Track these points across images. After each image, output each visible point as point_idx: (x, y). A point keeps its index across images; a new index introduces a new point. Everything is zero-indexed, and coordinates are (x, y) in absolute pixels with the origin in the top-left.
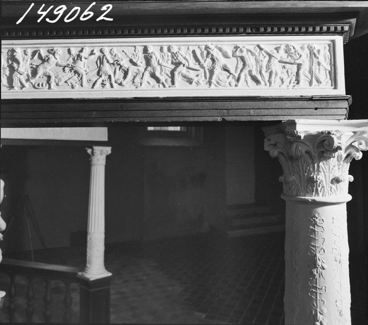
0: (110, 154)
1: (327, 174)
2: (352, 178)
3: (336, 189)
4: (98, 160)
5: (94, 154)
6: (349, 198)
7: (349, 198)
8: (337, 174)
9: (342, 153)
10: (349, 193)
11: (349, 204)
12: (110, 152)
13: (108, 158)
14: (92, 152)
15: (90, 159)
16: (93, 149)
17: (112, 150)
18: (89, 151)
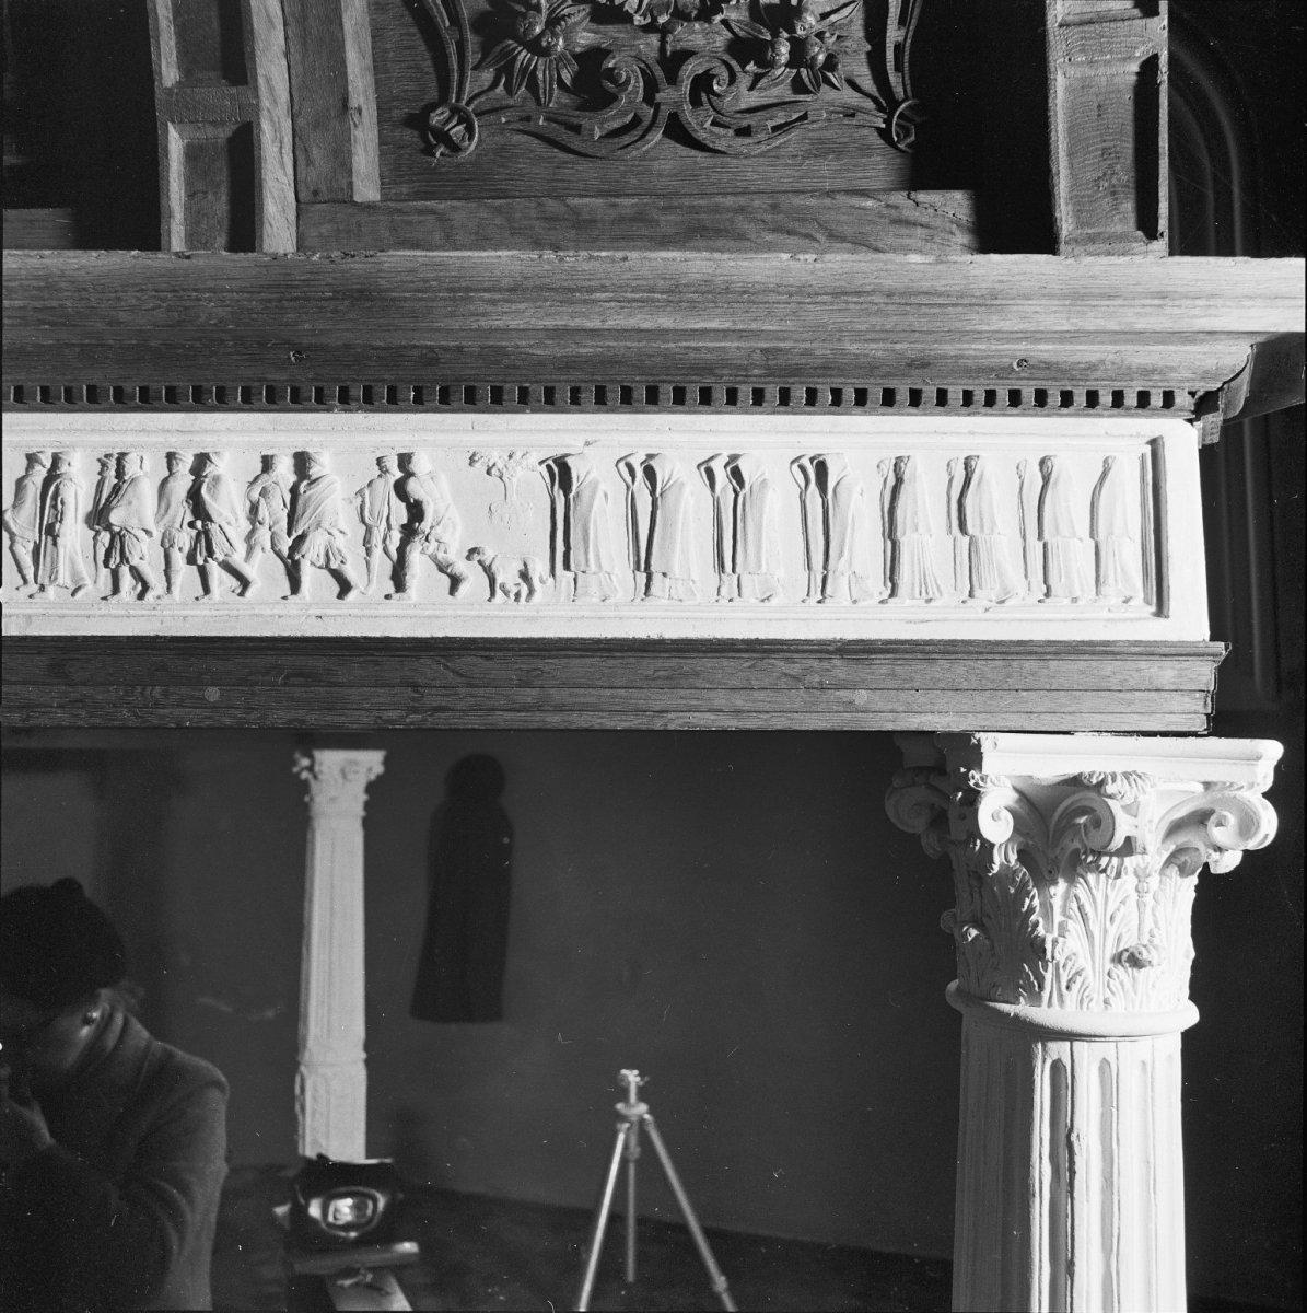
0: (379, 777)
1: (1095, 929)
3: (1128, 985)
4: (333, 799)
9: (1155, 851)
11: (1188, 1036)
12: (379, 769)
13: (371, 788)
14: (310, 769)
15: (307, 799)
16: (311, 757)
17: (386, 762)
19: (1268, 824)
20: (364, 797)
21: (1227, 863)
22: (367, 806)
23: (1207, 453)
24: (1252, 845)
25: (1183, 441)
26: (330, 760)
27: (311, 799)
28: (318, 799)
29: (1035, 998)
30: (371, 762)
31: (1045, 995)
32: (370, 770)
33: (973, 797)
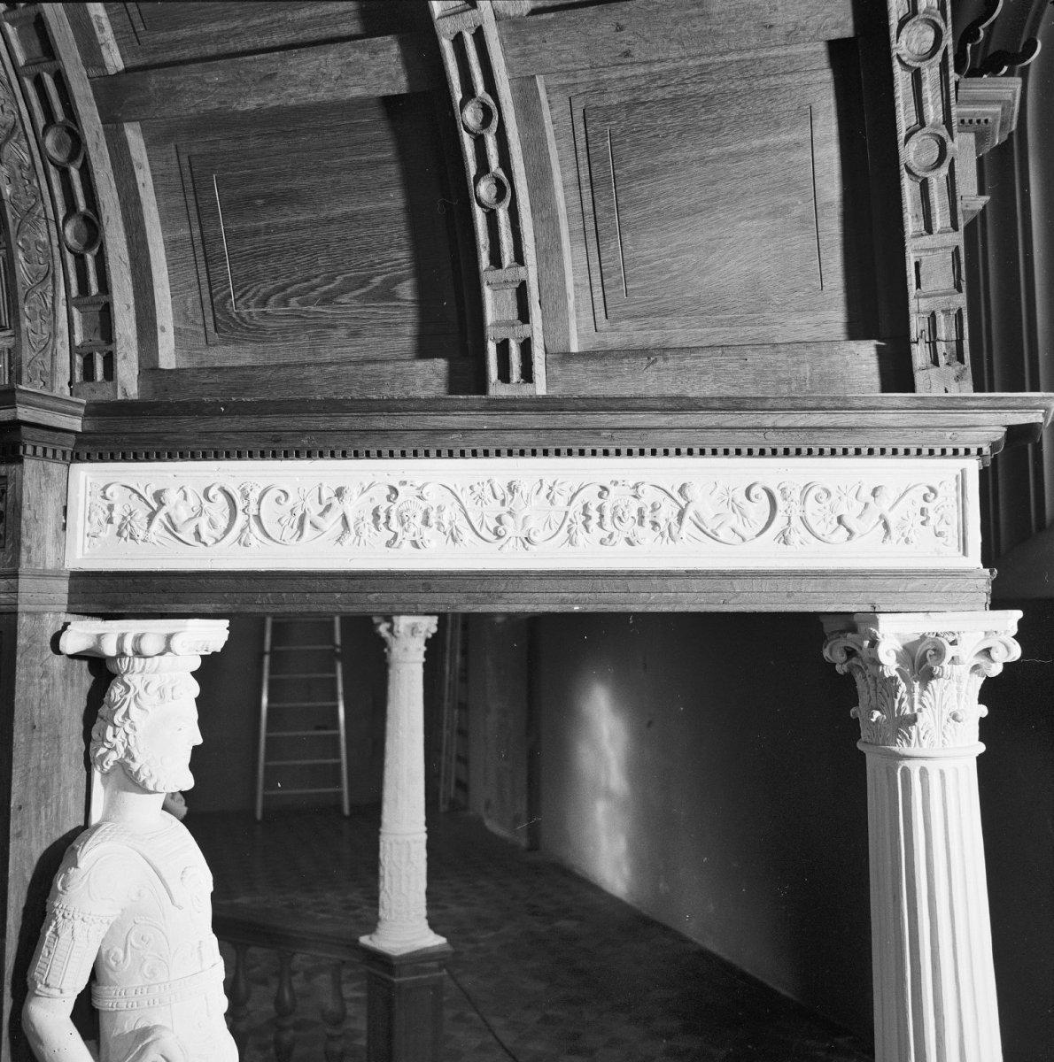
0: (433, 635)
2: (983, 711)
3: (953, 730)
5: (397, 634)
6: (982, 748)
7: (982, 748)
8: (953, 706)
9: (963, 670)
10: (981, 739)
11: (980, 759)
12: (434, 630)
13: (428, 642)
14: (391, 630)
15: (386, 650)
16: (392, 624)
18: (383, 629)
19: (1016, 652)
20: (424, 649)
21: (996, 670)
22: (426, 655)
23: (983, 474)
24: (1009, 660)
25: (973, 466)
26: (403, 622)
27: (389, 650)
28: (395, 650)
29: (909, 743)
30: (429, 625)
31: (913, 742)
32: (428, 631)
33: (874, 643)
